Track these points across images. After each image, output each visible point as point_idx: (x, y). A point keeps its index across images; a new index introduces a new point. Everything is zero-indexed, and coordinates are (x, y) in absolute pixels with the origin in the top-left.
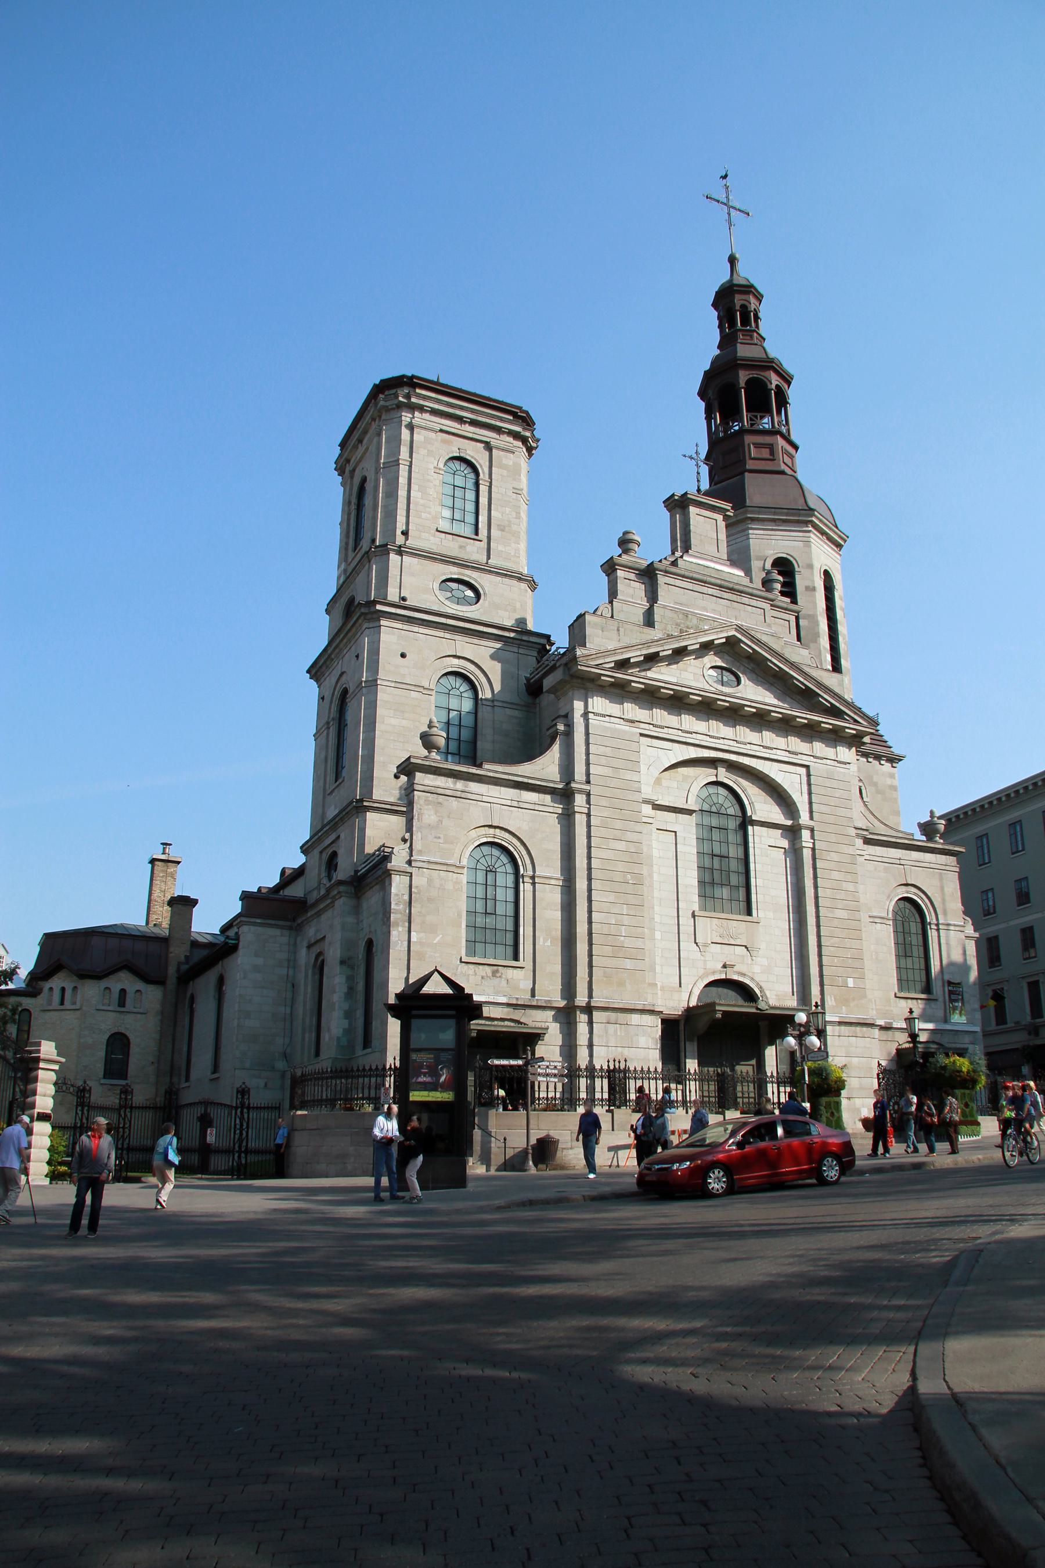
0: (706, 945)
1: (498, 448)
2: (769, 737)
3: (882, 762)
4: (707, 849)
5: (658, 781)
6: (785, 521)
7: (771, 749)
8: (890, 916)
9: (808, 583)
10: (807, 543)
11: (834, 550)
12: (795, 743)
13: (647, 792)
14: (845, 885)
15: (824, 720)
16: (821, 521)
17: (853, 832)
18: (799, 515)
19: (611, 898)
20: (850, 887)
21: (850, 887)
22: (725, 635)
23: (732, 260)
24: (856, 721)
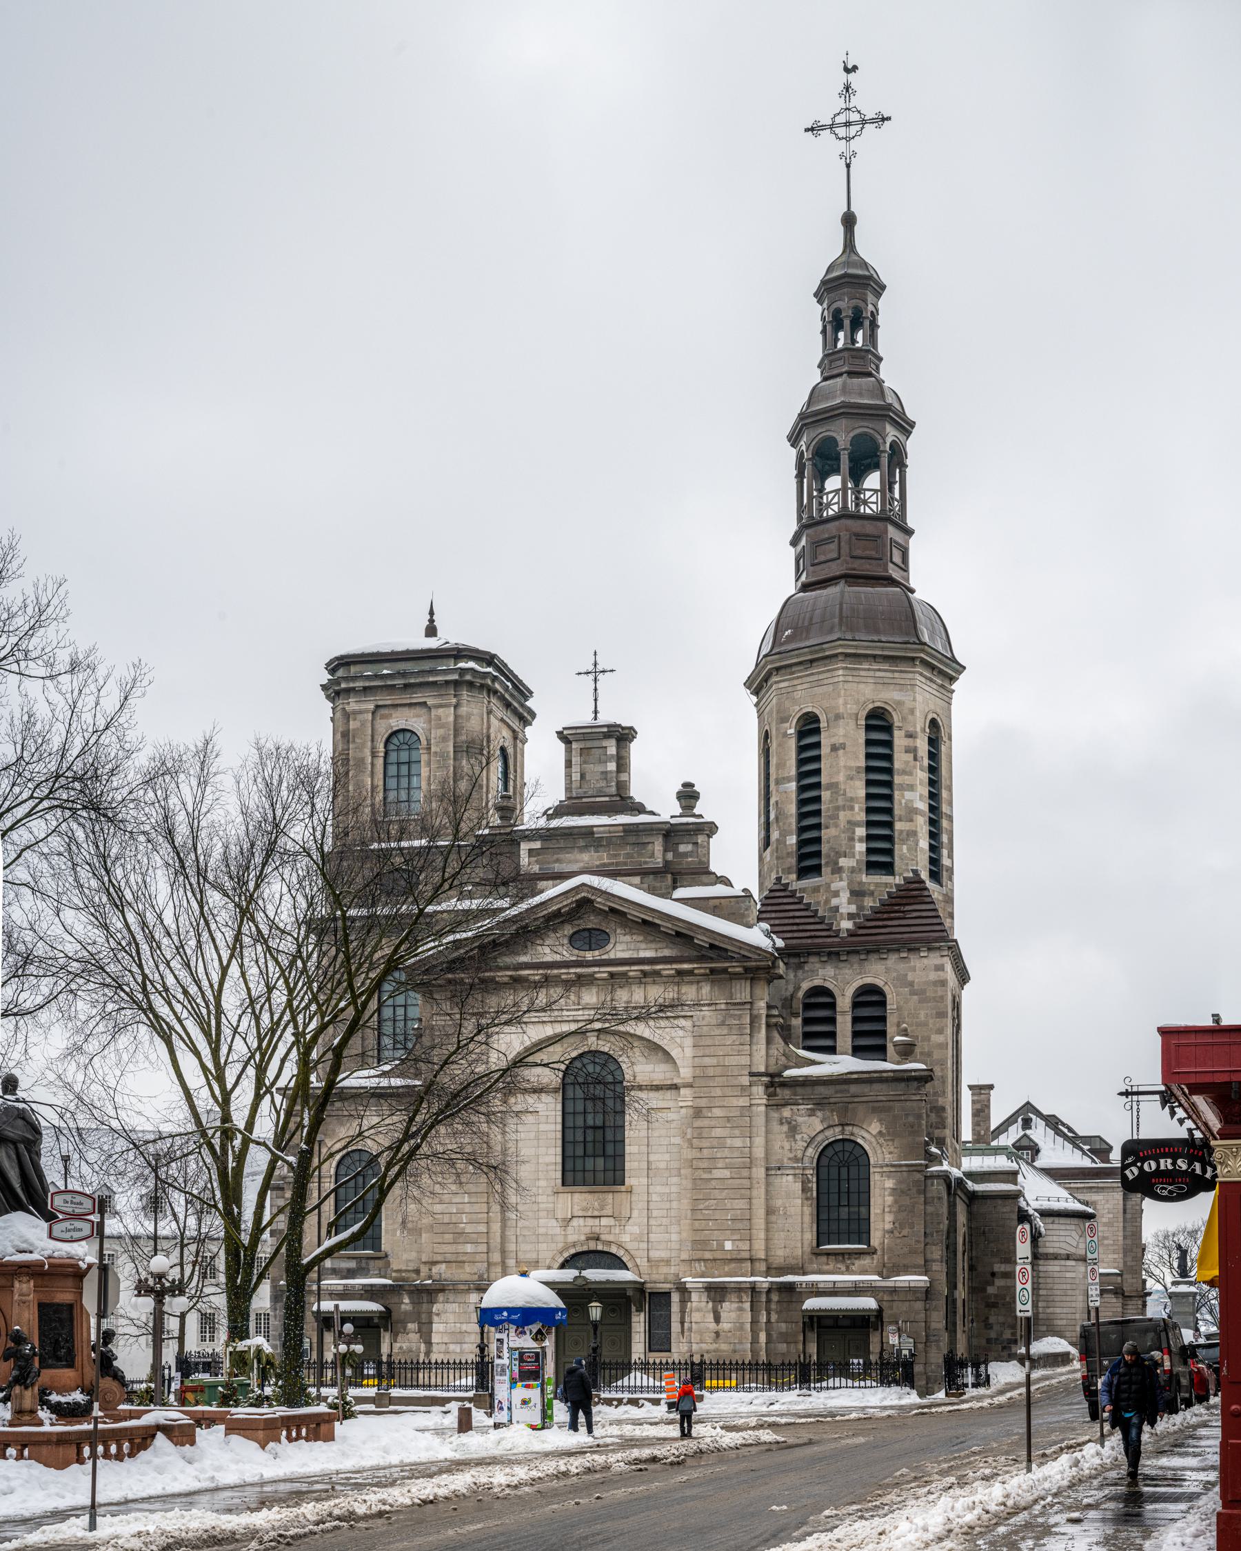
4: (580, 1121)
14: (729, 1141)
17: (745, 1080)
18: (824, 650)
20: (738, 1143)
21: (738, 1143)
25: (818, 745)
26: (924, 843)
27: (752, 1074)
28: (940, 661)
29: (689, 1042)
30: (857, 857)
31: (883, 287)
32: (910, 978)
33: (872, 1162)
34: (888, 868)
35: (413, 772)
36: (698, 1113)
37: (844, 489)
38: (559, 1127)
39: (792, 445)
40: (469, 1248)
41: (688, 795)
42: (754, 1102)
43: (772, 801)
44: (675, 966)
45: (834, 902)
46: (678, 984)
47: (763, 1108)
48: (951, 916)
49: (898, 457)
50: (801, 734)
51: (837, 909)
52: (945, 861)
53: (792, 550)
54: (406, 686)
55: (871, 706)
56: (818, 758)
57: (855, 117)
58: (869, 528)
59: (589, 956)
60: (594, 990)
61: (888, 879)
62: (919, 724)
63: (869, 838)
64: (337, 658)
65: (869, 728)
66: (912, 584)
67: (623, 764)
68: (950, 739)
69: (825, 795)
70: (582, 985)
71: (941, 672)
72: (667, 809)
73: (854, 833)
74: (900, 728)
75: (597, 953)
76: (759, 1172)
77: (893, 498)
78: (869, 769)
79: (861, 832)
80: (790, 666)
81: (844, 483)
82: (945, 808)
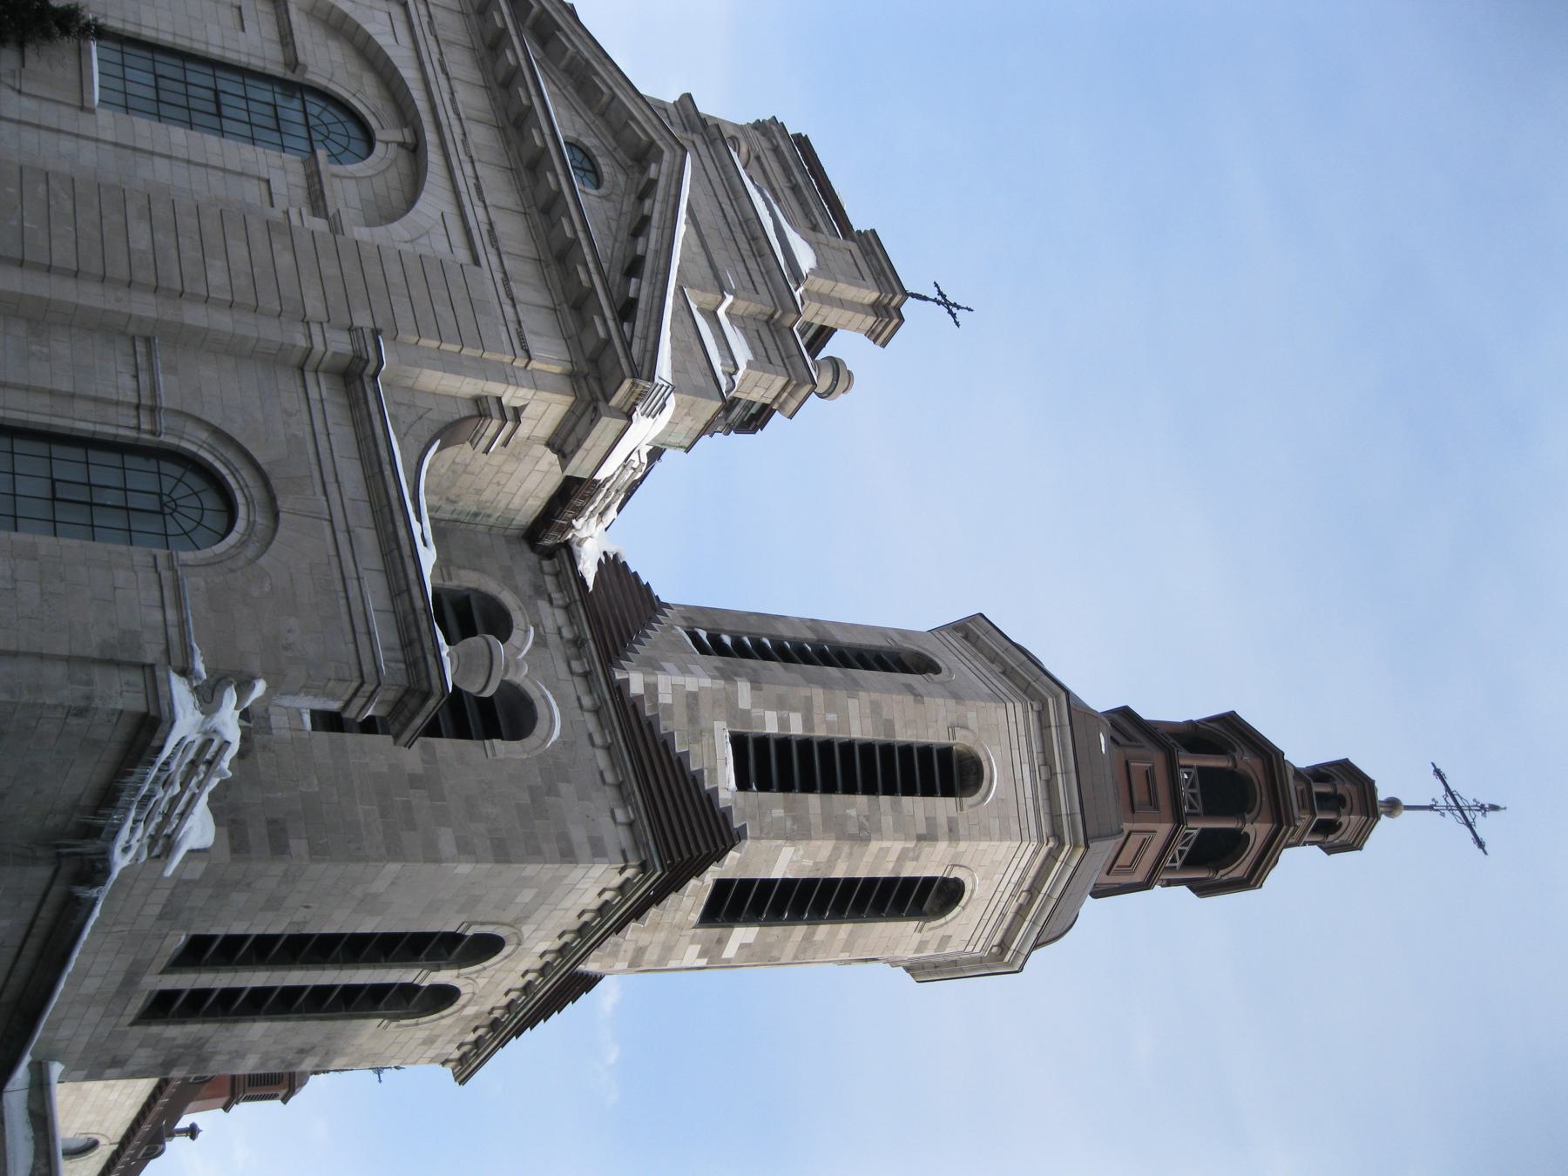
3: (620, 815)
11: (1037, 811)
15: (591, 266)
16: (1060, 726)
22: (655, 136)
23: (1393, 806)
24: (630, 345)
30: (756, 712)
32: (564, 788)
42: (315, 329)
44: (581, 235)
47: (302, 342)
55: (983, 757)
63: (784, 743)
70: (502, 129)
73: (795, 710)
76: (145, 307)
79: (796, 729)
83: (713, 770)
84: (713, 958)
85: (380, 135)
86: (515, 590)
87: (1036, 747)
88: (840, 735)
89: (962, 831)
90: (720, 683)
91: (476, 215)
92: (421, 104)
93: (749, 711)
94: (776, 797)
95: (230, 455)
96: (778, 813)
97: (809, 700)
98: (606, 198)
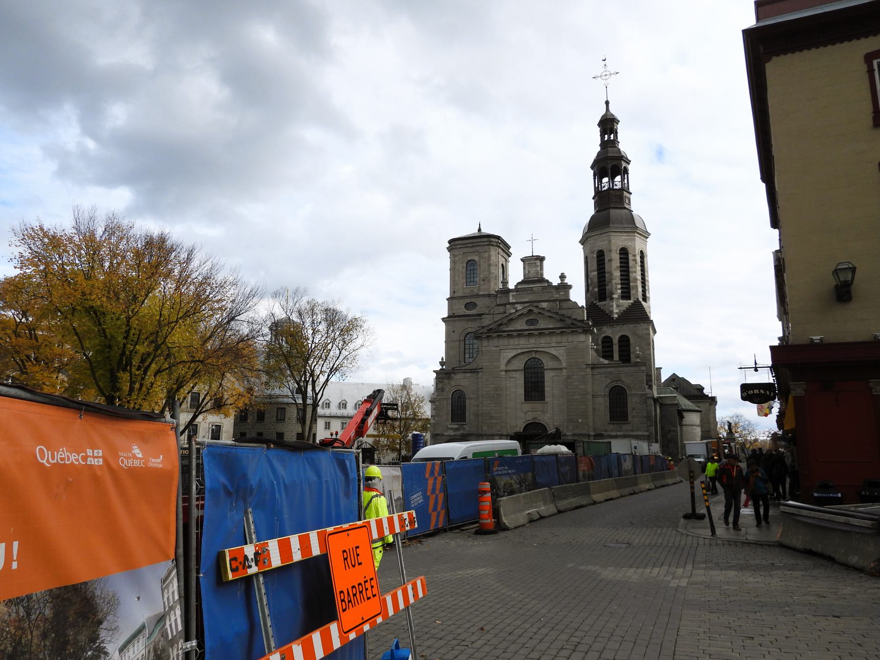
0: (527, 412)
1: (482, 252)
2: (548, 339)
5: (509, 361)
6: (601, 234)
7: (550, 343)
8: (608, 394)
9: (609, 258)
10: (610, 241)
12: (559, 338)
13: (503, 367)
17: (585, 366)
19: (489, 402)
20: (582, 387)
23: (607, 103)
25: (604, 260)
26: (640, 289)
27: (587, 365)
28: (642, 232)
29: (565, 354)
31: (619, 121)
32: (637, 332)
33: (628, 393)
34: (629, 298)
35: (475, 272)
36: (568, 377)
37: (609, 181)
38: (523, 382)
39: (592, 169)
40: (494, 421)
41: (562, 277)
43: (589, 278)
44: (560, 330)
45: (611, 309)
46: (561, 336)
48: (650, 312)
49: (626, 171)
50: (598, 256)
51: (612, 312)
52: (647, 295)
53: (593, 200)
54: (472, 247)
55: (621, 247)
56: (604, 264)
57: (608, 73)
58: (618, 193)
59: (532, 327)
60: (534, 338)
61: (629, 301)
62: (637, 252)
63: (622, 288)
64: (453, 239)
65: (620, 254)
66: (632, 209)
67: (542, 268)
68: (647, 256)
69: (607, 275)
71: (643, 236)
72: (556, 281)
74: (631, 254)
75: (534, 326)
76: (590, 397)
77: (625, 184)
78: (621, 267)
79: (619, 286)
80: (594, 236)
81: (609, 179)
82: (646, 278)
83: (629, 303)
84: (649, 298)
85: (534, 356)
86: (601, 334)
87: (618, 234)
88: (620, 278)
89: (634, 253)
90: (614, 301)
91: (554, 345)
92: (527, 350)
93: (618, 296)
94: (631, 291)
95: (609, 386)
96: (634, 291)
97: (615, 283)
98: (540, 320)
